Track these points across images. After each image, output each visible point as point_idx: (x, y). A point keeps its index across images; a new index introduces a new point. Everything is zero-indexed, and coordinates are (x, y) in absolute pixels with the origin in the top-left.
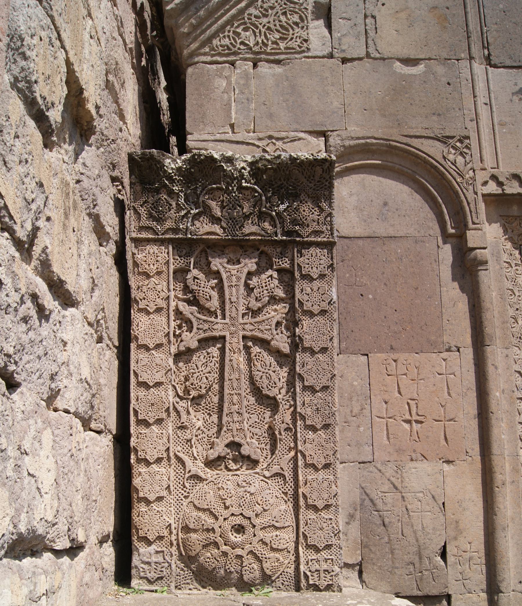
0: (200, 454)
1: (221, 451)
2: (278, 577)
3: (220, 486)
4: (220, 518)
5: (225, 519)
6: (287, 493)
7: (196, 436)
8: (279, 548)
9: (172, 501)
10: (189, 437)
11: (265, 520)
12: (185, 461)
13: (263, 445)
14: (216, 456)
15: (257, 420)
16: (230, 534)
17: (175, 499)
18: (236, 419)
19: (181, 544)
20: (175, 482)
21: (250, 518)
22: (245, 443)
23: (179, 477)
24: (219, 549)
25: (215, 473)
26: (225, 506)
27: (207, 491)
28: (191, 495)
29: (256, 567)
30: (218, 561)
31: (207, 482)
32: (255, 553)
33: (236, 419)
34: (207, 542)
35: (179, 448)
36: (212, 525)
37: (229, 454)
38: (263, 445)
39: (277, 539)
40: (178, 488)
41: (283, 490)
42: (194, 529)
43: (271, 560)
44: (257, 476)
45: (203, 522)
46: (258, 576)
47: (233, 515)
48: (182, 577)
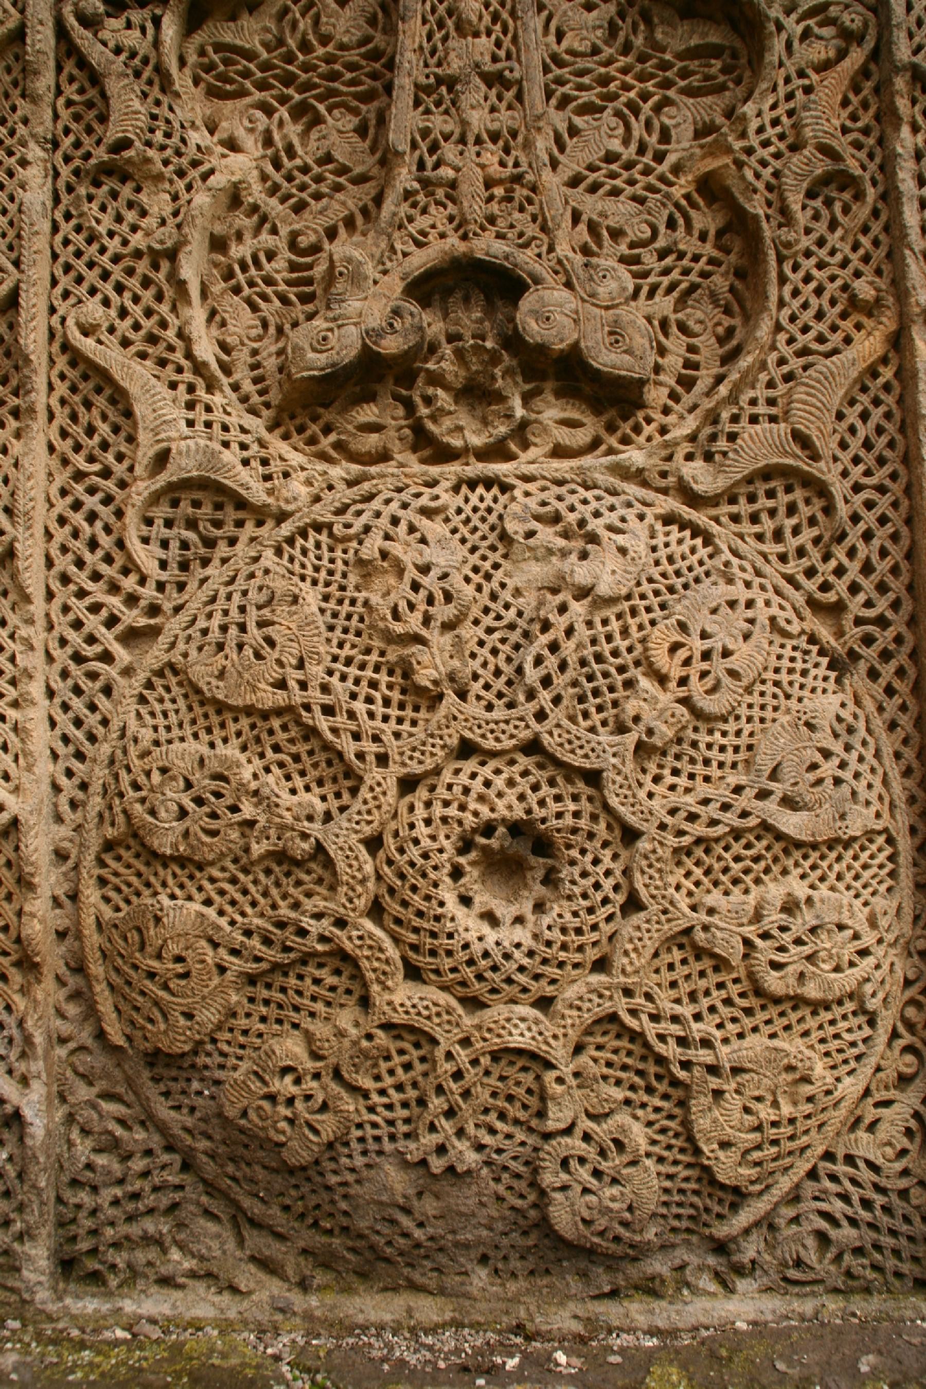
0: (243, 357)
1: (376, 317)
2: (794, 1198)
3: (372, 546)
4: (373, 774)
5: (408, 785)
6: (839, 608)
7: (218, 244)
8: (812, 991)
9: (34, 661)
10: (166, 236)
11: (703, 789)
12: (134, 389)
13: (664, 305)
14: (350, 354)
15: (615, 145)
16: (448, 894)
17: (62, 656)
18: (478, 119)
19: (97, 969)
20: (61, 534)
21: (593, 778)
22: (540, 269)
23: (92, 502)
24: (365, 1002)
25: (337, 472)
26: (410, 688)
27: (279, 585)
28: (174, 626)
29: (639, 1135)
30: (354, 1089)
31: (286, 529)
32: (636, 1036)
33: (478, 119)
34: (273, 955)
35: (93, 310)
36: (315, 829)
37: (433, 348)
38: (664, 305)
39: (799, 924)
40: (82, 578)
41: (811, 585)
42: (182, 861)
43: (754, 1084)
44: (633, 490)
45: (248, 810)
46: (651, 1199)
47: (466, 749)
48: (108, 1193)
